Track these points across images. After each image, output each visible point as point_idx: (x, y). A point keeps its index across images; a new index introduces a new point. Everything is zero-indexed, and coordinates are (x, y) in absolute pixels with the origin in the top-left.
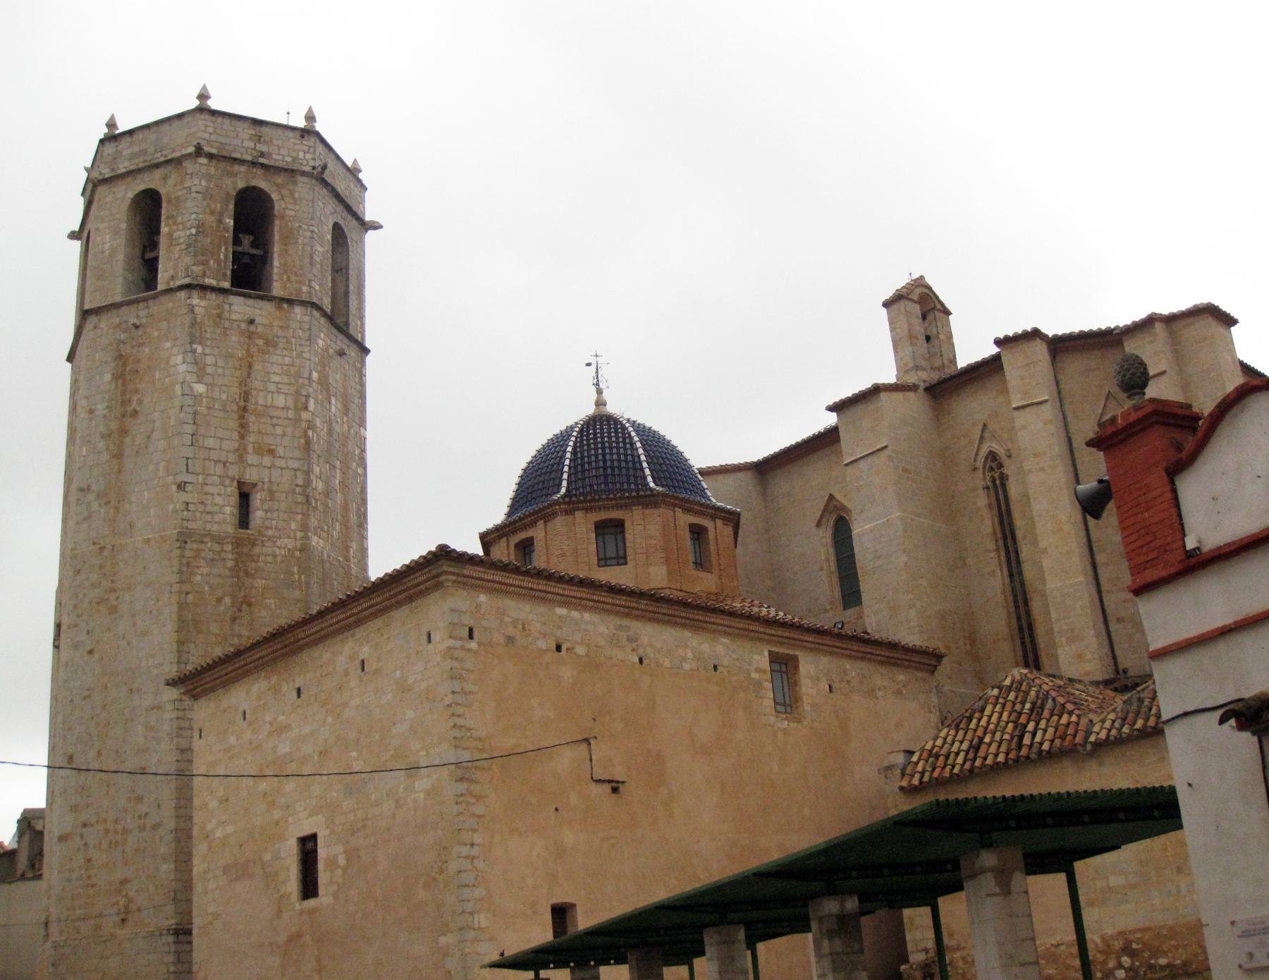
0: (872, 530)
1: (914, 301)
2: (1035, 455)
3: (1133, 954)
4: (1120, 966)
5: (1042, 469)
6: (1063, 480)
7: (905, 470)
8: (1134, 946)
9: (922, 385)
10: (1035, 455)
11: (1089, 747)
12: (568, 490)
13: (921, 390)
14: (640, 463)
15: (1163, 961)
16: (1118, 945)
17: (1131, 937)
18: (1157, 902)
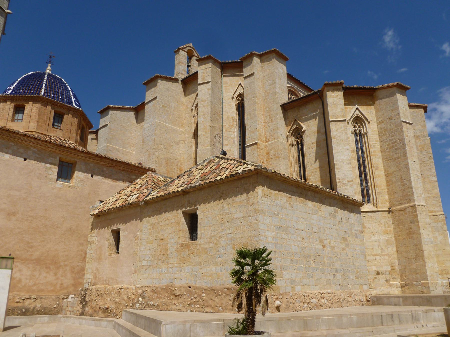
0: (148, 126)
1: (185, 51)
2: (202, 101)
3: (143, 297)
4: (138, 302)
5: (204, 106)
6: (210, 111)
7: (163, 106)
8: (144, 294)
9: (180, 80)
10: (202, 101)
11: (143, 203)
12: (11, 93)
13: (180, 82)
14: (42, 87)
15: (151, 303)
16: (139, 292)
17: (144, 289)
18: (155, 275)
